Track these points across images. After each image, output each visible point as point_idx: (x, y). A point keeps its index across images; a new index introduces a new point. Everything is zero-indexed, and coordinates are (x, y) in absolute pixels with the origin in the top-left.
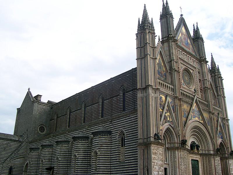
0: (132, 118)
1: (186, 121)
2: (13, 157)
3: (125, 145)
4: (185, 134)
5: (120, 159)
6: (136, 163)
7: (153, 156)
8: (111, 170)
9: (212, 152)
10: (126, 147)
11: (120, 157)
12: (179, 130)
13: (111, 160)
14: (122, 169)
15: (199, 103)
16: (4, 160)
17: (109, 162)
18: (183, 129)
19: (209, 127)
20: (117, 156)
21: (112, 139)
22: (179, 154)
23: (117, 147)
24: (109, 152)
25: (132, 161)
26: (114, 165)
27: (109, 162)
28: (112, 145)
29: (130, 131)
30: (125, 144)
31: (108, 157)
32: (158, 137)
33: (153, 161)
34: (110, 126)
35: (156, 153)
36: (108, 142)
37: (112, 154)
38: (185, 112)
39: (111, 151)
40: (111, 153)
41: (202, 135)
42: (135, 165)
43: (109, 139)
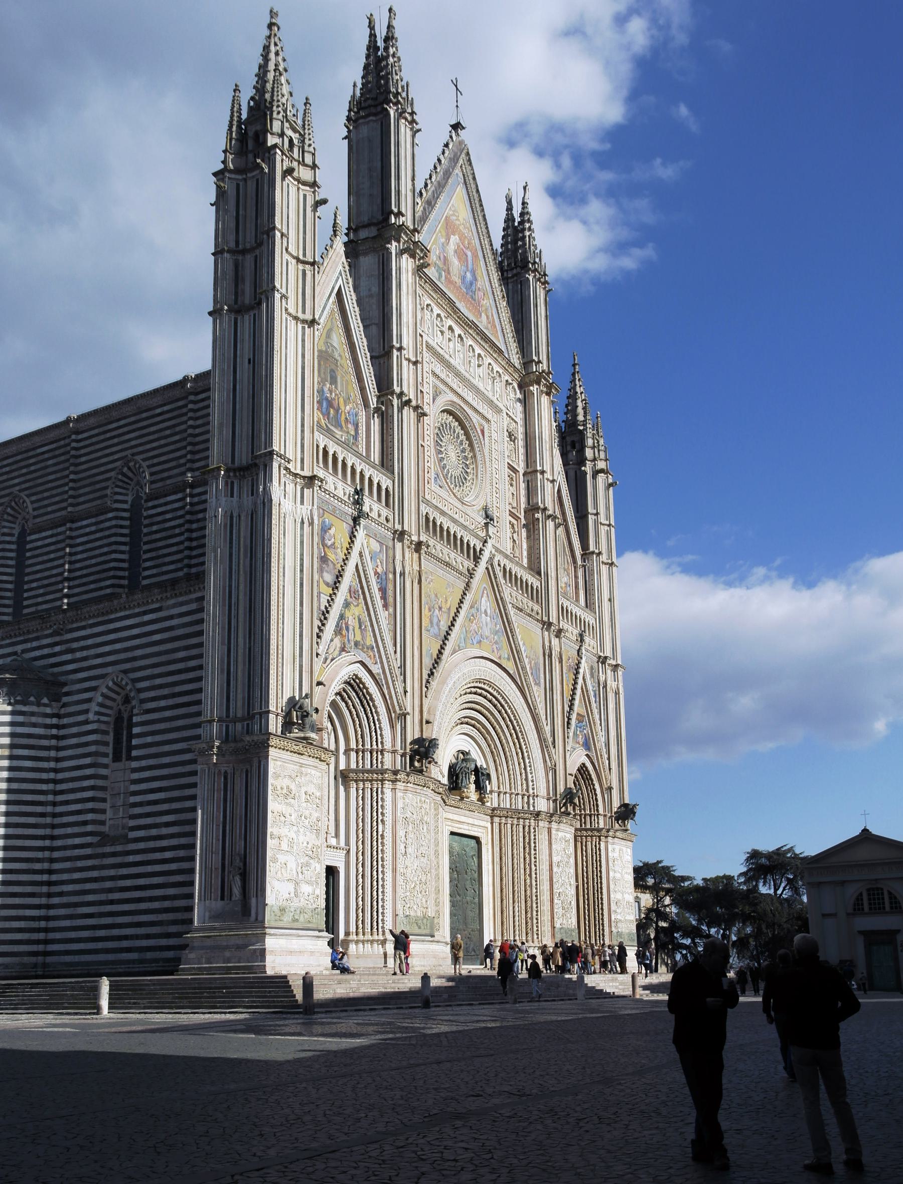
0: (171, 617)
1: (440, 653)
3: (134, 753)
4: (429, 712)
5: (102, 823)
6: (183, 841)
8: (54, 878)
10: (135, 764)
11: (103, 811)
12: (405, 692)
13: (53, 826)
14: (112, 872)
17: (43, 838)
18: (424, 689)
19: (538, 693)
20: (90, 805)
21: (65, 721)
22: (400, 805)
23: (88, 761)
24: (44, 787)
25: (164, 831)
26: (68, 853)
27: (43, 838)
28: (62, 754)
29: (158, 681)
30: (130, 748)
31: (39, 809)
32: (305, 715)
34: (54, 655)
35: (288, 794)
36: (40, 737)
37: (60, 798)
38: (437, 611)
39: (55, 782)
40: (56, 793)
41: (502, 723)
42: (181, 853)
43: (48, 721)
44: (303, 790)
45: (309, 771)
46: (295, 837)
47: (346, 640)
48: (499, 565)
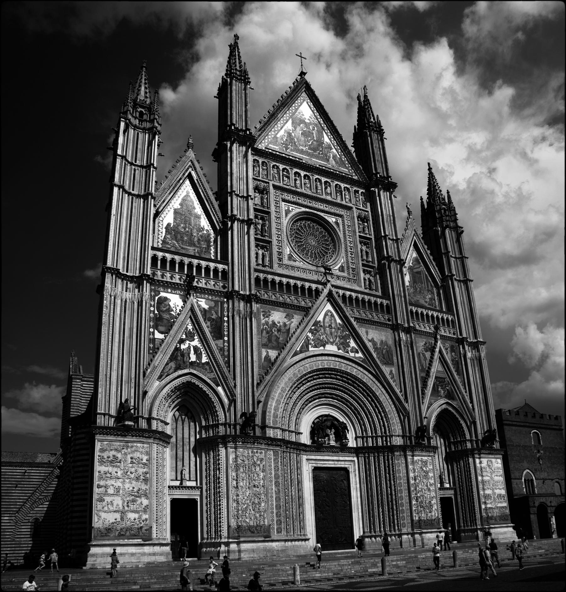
2: (38, 498)
7: (98, 468)
9: (398, 441)
15: (340, 301)
16: (18, 506)
33: (102, 483)
35: (114, 461)
44: (129, 457)
45: (135, 444)
46: (120, 485)
47: (181, 363)
48: (339, 296)
